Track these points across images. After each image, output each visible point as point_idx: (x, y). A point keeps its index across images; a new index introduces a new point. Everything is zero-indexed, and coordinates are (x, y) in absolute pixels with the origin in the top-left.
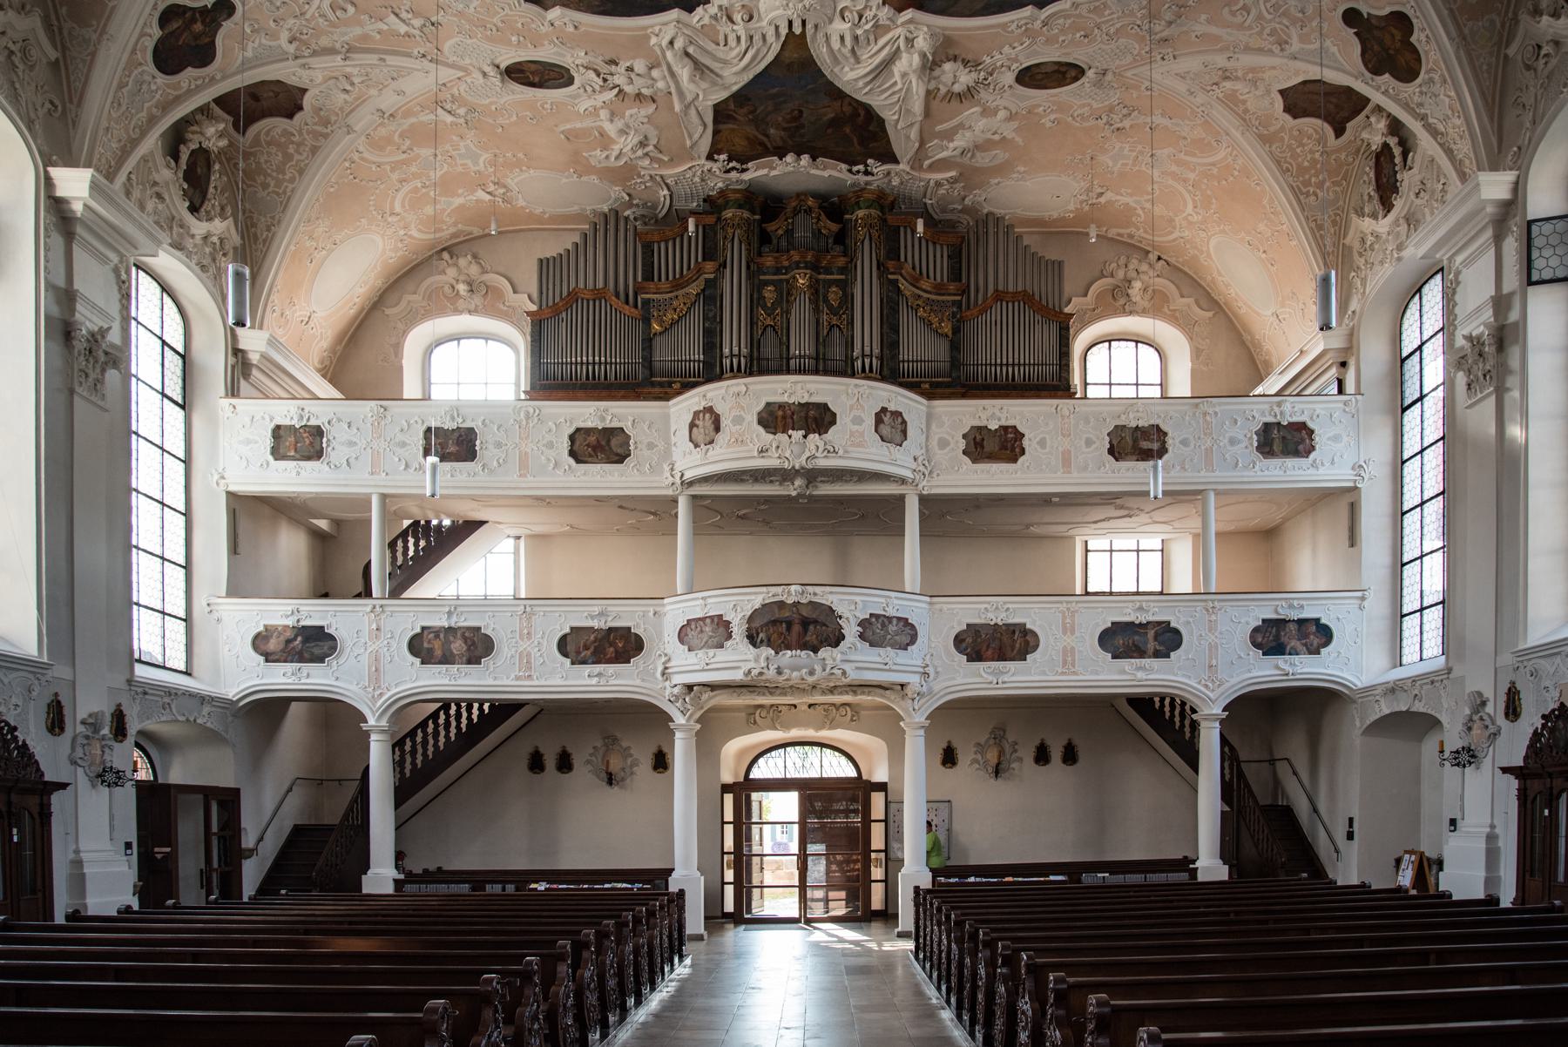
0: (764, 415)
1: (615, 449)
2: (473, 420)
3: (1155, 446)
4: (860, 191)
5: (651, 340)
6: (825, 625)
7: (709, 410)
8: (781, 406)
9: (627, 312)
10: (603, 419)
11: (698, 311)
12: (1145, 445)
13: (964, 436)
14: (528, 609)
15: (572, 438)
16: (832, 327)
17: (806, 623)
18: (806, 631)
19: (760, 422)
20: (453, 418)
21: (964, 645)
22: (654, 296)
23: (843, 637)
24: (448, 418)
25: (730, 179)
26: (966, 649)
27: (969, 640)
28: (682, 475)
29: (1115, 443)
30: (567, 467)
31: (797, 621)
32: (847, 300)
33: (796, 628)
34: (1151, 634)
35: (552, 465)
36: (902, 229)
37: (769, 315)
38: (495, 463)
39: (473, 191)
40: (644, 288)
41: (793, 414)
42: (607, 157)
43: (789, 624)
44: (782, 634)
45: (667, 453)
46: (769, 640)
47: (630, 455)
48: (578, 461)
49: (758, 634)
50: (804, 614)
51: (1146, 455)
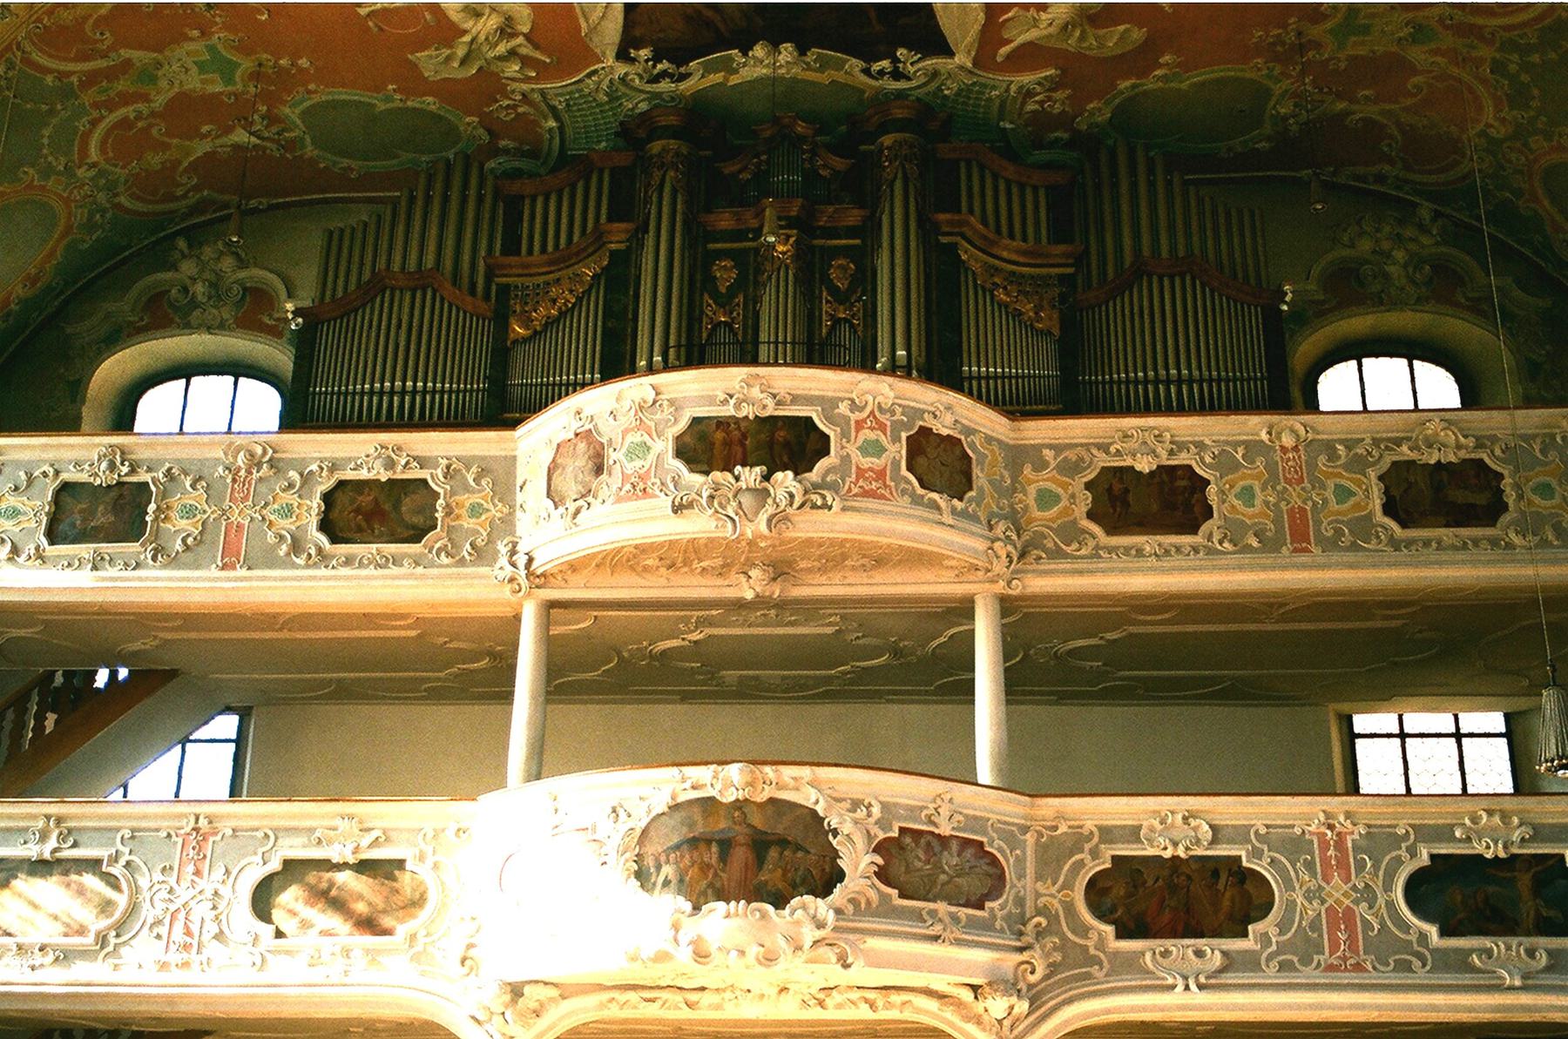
0: (687, 439)
1: (407, 518)
2: (149, 470)
3: (1481, 499)
4: (883, 101)
5: (507, 351)
6: (799, 848)
7: (586, 436)
8: (722, 423)
9: (469, 308)
10: (390, 464)
11: (595, 306)
12: (1459, 496)
13: (1088, 486)
14: (203, 822)
15: (328, 498)
16: (837, 322)
17: (761, 845)
18: (760, 859)
19: (680, 453)
20: (112, 467)
21: (1108, 902)
22: (519, 281)
23: (840, 876)
24: (104, 465)
25: (658, 95)
26: (1113, 910)
27: (1119, 890)
28: (531, 560)
29: (1395, 493)
30: (313, 552)
31: (741, 839)
32: (865, 279)
33: (740, 855)
34: (1524, 881)
35: (284, 547)
36: (963, 164)
37: (722, 306)
38: (178, 546)
39: (229, 130)
40: (503, 267)
41: (744, 436)
42: (448, 59)
43: (726, 845)
44: (709, 866)
45: (508, 523)
46: (681, 881)
47: (435, 527)
48: (334, 540)
49: (659, 868)
50: (760, 827)
51: (1461, 516)
